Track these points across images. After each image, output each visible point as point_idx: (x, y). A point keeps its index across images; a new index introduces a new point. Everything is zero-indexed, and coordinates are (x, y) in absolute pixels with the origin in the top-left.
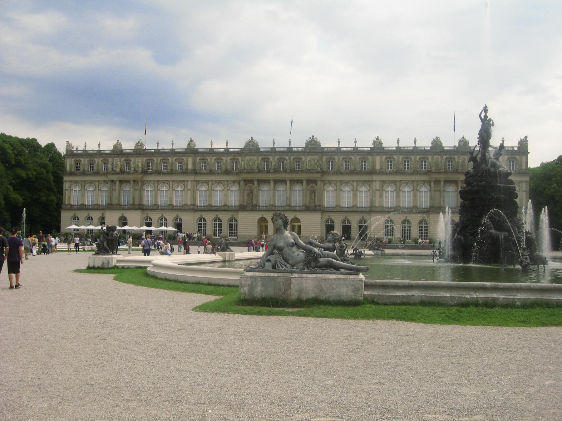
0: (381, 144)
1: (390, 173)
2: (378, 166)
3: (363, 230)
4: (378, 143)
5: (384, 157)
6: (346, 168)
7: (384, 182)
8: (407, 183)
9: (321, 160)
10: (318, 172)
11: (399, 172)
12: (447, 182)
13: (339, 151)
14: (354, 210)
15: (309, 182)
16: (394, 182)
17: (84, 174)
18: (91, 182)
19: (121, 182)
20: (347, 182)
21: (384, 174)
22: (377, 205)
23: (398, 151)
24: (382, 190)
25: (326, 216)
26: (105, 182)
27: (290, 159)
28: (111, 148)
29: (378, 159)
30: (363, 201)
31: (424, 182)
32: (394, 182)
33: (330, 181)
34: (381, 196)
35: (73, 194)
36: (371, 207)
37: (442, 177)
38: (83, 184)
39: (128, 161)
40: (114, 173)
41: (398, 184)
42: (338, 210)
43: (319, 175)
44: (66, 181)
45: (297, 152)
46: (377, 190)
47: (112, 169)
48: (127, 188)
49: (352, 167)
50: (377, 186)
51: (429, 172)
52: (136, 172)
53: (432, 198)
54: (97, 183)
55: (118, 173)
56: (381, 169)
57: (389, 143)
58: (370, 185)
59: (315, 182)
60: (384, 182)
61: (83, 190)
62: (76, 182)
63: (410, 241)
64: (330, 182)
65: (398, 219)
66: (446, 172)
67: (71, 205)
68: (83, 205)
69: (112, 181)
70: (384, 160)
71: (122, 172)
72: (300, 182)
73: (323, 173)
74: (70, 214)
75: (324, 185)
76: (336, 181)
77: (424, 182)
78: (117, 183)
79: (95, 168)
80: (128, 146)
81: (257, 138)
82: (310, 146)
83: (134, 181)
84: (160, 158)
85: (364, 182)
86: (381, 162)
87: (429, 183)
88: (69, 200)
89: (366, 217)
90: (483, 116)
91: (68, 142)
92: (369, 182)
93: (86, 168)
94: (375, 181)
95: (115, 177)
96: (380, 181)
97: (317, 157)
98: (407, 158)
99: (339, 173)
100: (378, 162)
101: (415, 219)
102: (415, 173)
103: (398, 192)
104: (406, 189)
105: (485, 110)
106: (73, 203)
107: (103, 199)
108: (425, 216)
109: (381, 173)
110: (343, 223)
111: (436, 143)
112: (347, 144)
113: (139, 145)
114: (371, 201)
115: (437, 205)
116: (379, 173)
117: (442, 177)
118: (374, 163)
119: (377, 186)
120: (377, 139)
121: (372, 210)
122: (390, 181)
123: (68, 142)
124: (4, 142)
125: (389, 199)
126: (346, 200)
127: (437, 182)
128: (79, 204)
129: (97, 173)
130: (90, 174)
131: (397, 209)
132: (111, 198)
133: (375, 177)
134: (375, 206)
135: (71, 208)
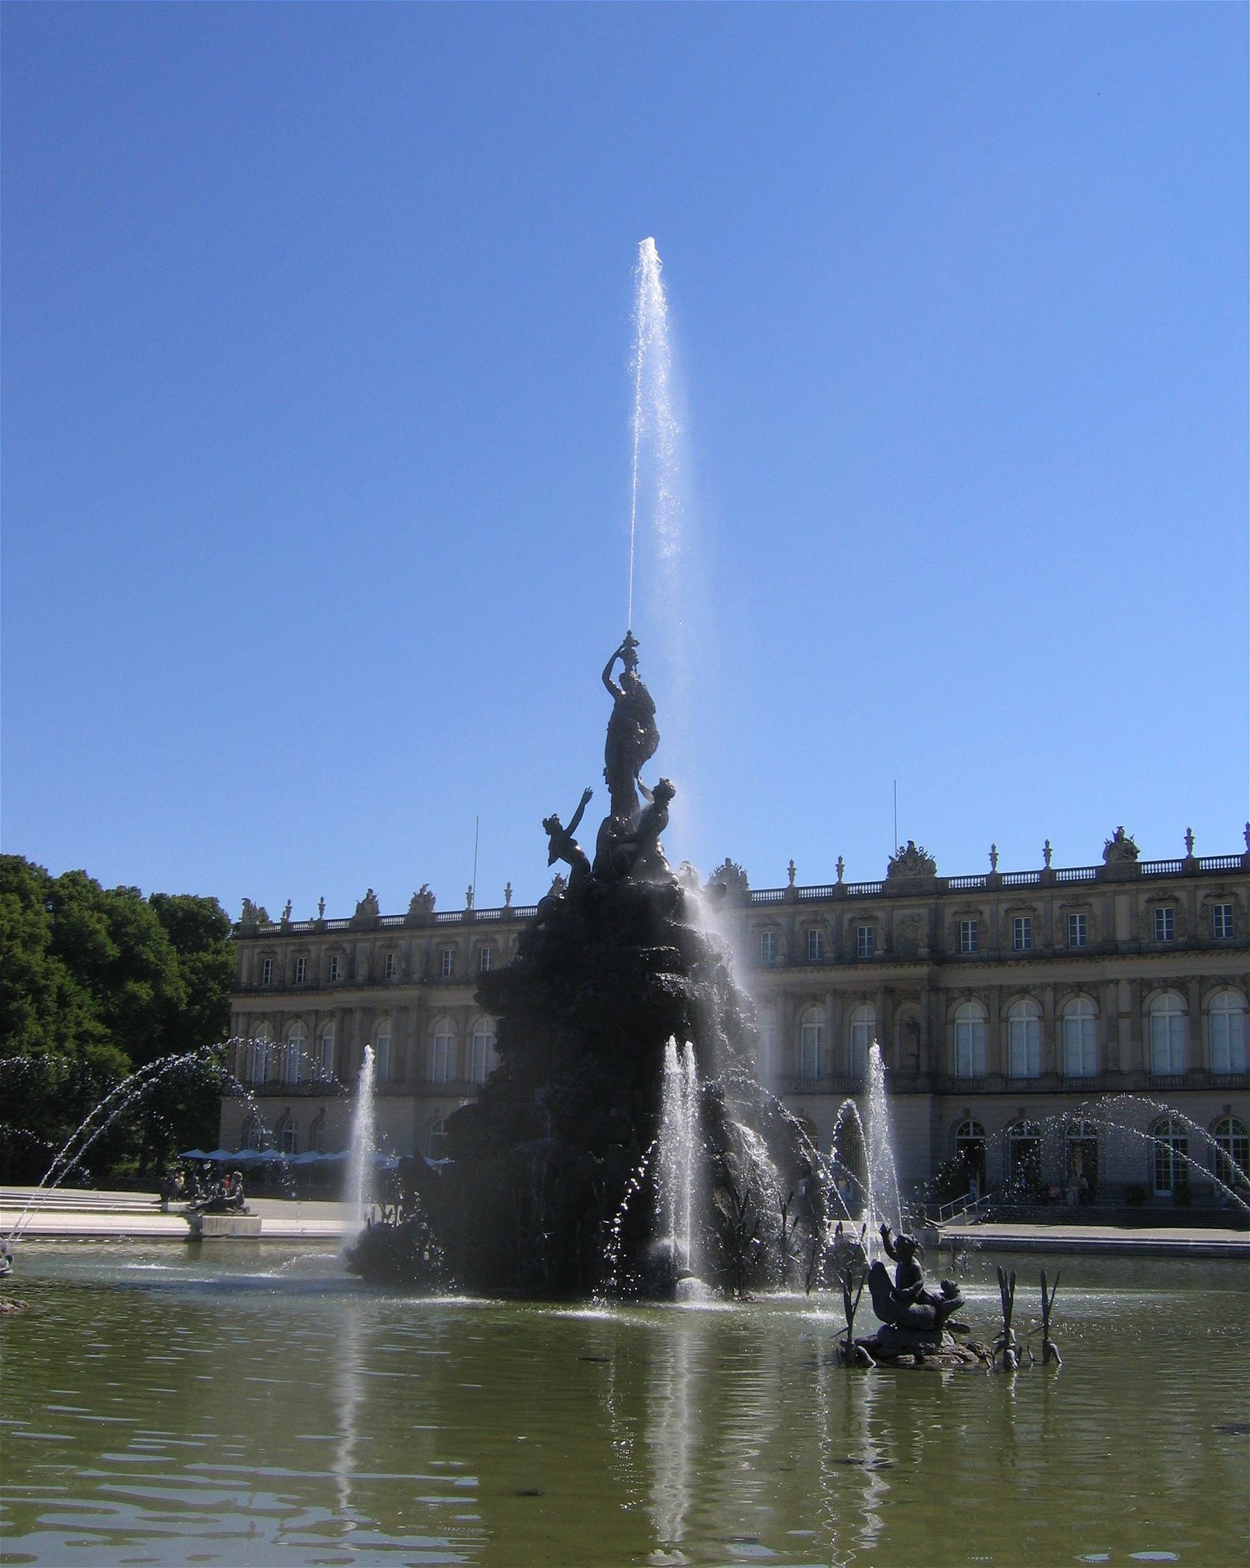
0: (1132, 851)
1: (1164, 952)
2: (1123, 933)
4: (1121, 849)
5: (1144, 897)
6: (1019, 943)
7: (1143, 987)
9: (936, 920)
10: (918, 961)
13: (993, 884)
16: (1180, 985)
17: (282, 990)
18: (297, 1016)
20: (1024, 991)
22: (1125, 1065)
24: (1141, 1014)
25: (956, 1107)
26: (331, 1014)
27: (839, 923)
28: (351, 913)
29: (1122, 904)
30: (1081, 1057)
32: (1180, 985)
33: (969, 989)
34: (1138, 1035)
36: (1104, 1073)
40: (351, 982)
41: (1193, 988)
42: (999, 1083)
43: (923, 971)
44: (238, 1014)
45: (861, 897)
46: (1120, 1015)
47: (351, 975)
49: (1039, 942)
54: (313, 1018)
55: (360, 987)
56: (1135, 939)
57: (1158, 849)
58: (1097, 999)
60: (1143, 987)
63: (1166, 1193)
64: (968, 993)
68: (275, 1082)
69: (347, 1011)
70: (1142, 906)
75: (949, 1002)
76: (984, 989)
78: (358, 1016)
79: (310, 975)
82: (899, 877)
83: (404, 1009)
84: (473, 938)
85: (1079, 988)
86: (1134, 914)
90: (615, 679)
91: (247, 902)
92: (1092, 989)
93: (289, 973)
94: (1117, 982)
96: (1131, 981)
98: (1220, 896)
100: (1123, 915)
105: (627, 652)
109: (1138, 951)
110: (961, 1133)
112: (1020, 861)
114: (1107, 1054)
120: (1119, 836)
122: (1165, 980)
123: (247, 902)
124: (97, 907)
128: (269, 1079)
130: (292, 992)
134: (1120, 1072)
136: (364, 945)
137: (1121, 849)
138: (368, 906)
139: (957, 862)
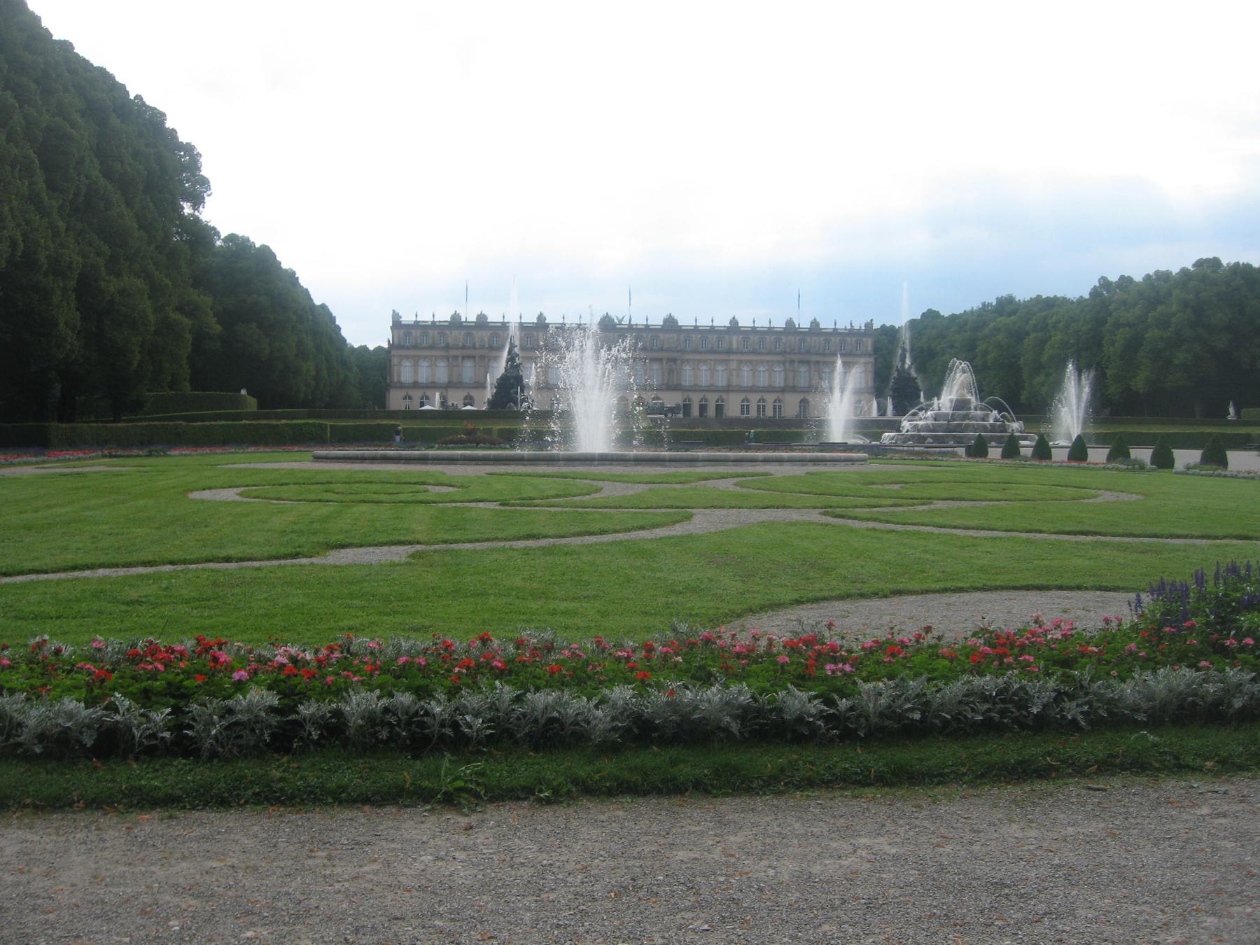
1: (747, 353)
2: (735, 346)
3: (719, 409)
4: (734, 321)
8: (762, 362)
11: (754, 352)
12: (800, 362)
14: (711, 389)
15: (669, 360)
16: (751, 362)
17: (416, 347)
18: (425, 358)
19: (464, 358)
20: (705, 361)
21: (742, 353)
23: (754, 330)
29: (735, 338)
30: (721, 381)
31: (779, 362)
34: (738, 375)
35: (405, 372)
37: (796, 358)
38: (416, 361)
39: (469, 334)
40: (457, 348)
42: (695, 388)
48: (468, 364)
50: (734, 365)
51: (783, 353)
52: (482, 347)
53: (786, 379)
57: (745, 322)
59: (674, 360)
60: (740, 362)
61: (416, 365)
62: (407, 357)
64: (688, 361)
65: (754, 398)
66: (800, 353)
67: (399, 382)
71: (464, 347)
72: (660, 360)
73: (683, 352)
74: (403, 393)
77: (779, 362)
80: (470, 316)
81: (612, 315)
85: (721, 361)
87: (784, 363)
88: (399, 376)
89: (724, 396)
95: (458, 353)
97: (675, 335)
99: (696, 352)
100: (735, 341)
101: (770, 398)
102: (769, 353)
103: (754, 371)
104: (761, 369)
106: (403, 379)
107: (442, 374)
108: (780, 395)
111: (790, 323)
112: (704, 322)
113: (482, 318)
114: (729, 380)
115: (791, 384)
116: (736, 353)
117: (796, 358)
118: (731, 344)
119: (734, 365)
121: (728, 389)
125: (746, 379)
126: (704, 380)
127: (792, 362)
129: (432, 347)
130: (424, 348)
131: (753, 389)
132: (450, 375)
133: (732, 357)
135: (402, 386)
136: (455, 333)
137: (734, 321)
138: (456, 317)
139: (685, 320)
